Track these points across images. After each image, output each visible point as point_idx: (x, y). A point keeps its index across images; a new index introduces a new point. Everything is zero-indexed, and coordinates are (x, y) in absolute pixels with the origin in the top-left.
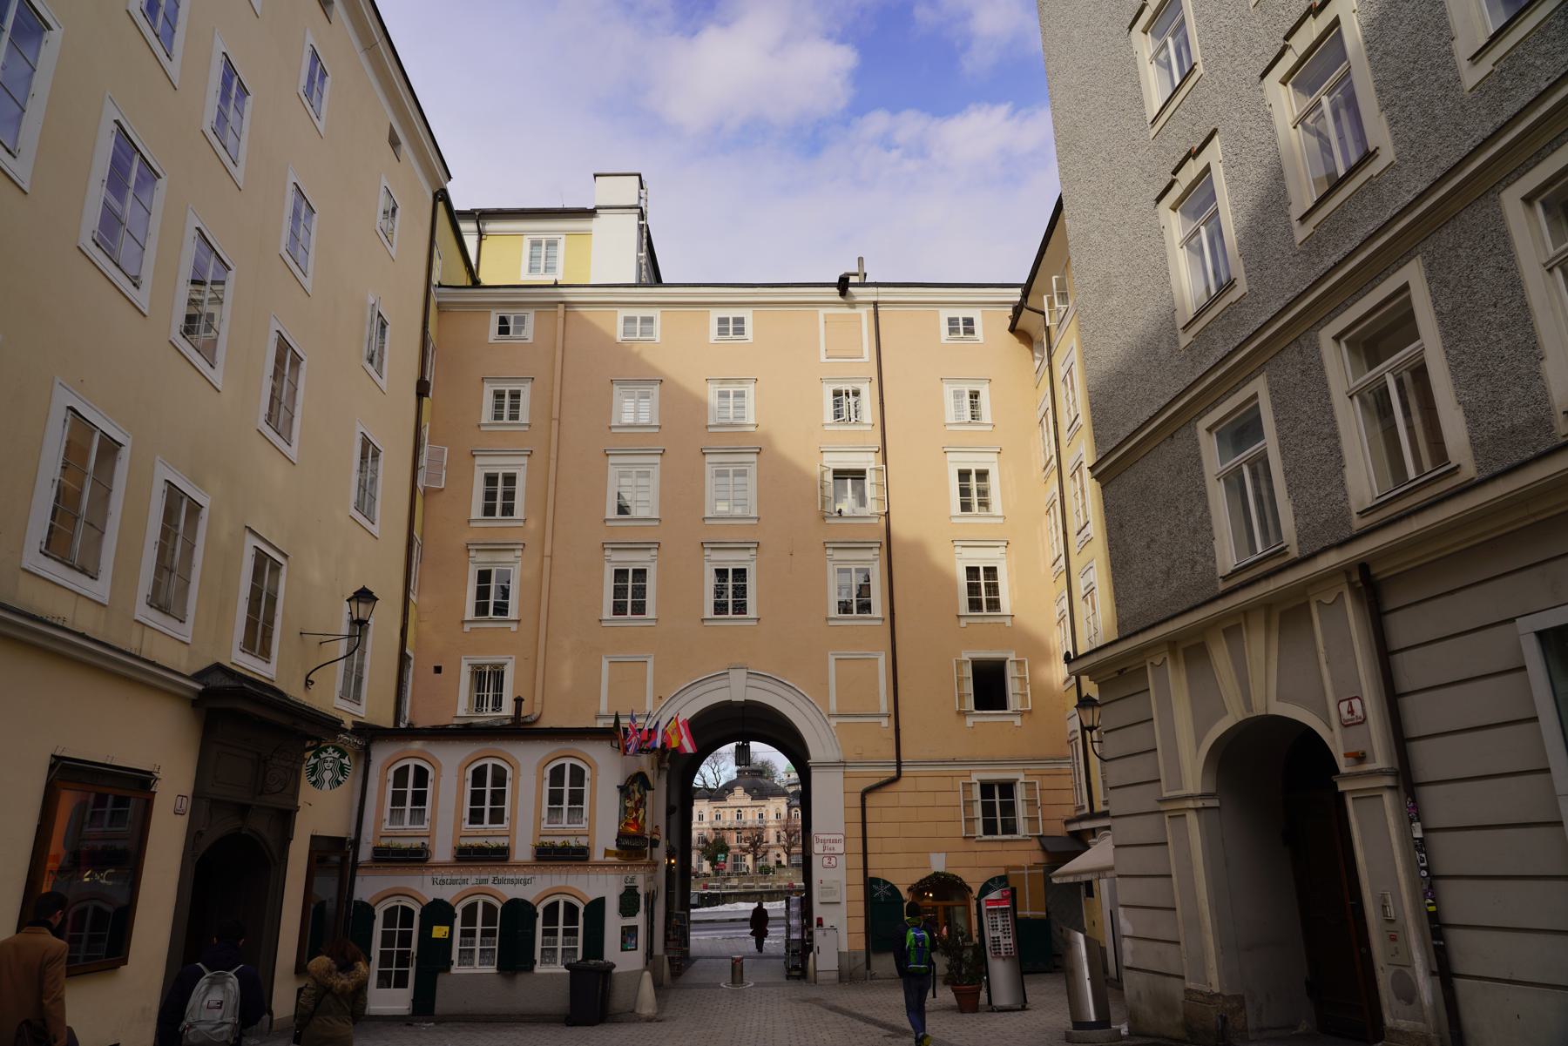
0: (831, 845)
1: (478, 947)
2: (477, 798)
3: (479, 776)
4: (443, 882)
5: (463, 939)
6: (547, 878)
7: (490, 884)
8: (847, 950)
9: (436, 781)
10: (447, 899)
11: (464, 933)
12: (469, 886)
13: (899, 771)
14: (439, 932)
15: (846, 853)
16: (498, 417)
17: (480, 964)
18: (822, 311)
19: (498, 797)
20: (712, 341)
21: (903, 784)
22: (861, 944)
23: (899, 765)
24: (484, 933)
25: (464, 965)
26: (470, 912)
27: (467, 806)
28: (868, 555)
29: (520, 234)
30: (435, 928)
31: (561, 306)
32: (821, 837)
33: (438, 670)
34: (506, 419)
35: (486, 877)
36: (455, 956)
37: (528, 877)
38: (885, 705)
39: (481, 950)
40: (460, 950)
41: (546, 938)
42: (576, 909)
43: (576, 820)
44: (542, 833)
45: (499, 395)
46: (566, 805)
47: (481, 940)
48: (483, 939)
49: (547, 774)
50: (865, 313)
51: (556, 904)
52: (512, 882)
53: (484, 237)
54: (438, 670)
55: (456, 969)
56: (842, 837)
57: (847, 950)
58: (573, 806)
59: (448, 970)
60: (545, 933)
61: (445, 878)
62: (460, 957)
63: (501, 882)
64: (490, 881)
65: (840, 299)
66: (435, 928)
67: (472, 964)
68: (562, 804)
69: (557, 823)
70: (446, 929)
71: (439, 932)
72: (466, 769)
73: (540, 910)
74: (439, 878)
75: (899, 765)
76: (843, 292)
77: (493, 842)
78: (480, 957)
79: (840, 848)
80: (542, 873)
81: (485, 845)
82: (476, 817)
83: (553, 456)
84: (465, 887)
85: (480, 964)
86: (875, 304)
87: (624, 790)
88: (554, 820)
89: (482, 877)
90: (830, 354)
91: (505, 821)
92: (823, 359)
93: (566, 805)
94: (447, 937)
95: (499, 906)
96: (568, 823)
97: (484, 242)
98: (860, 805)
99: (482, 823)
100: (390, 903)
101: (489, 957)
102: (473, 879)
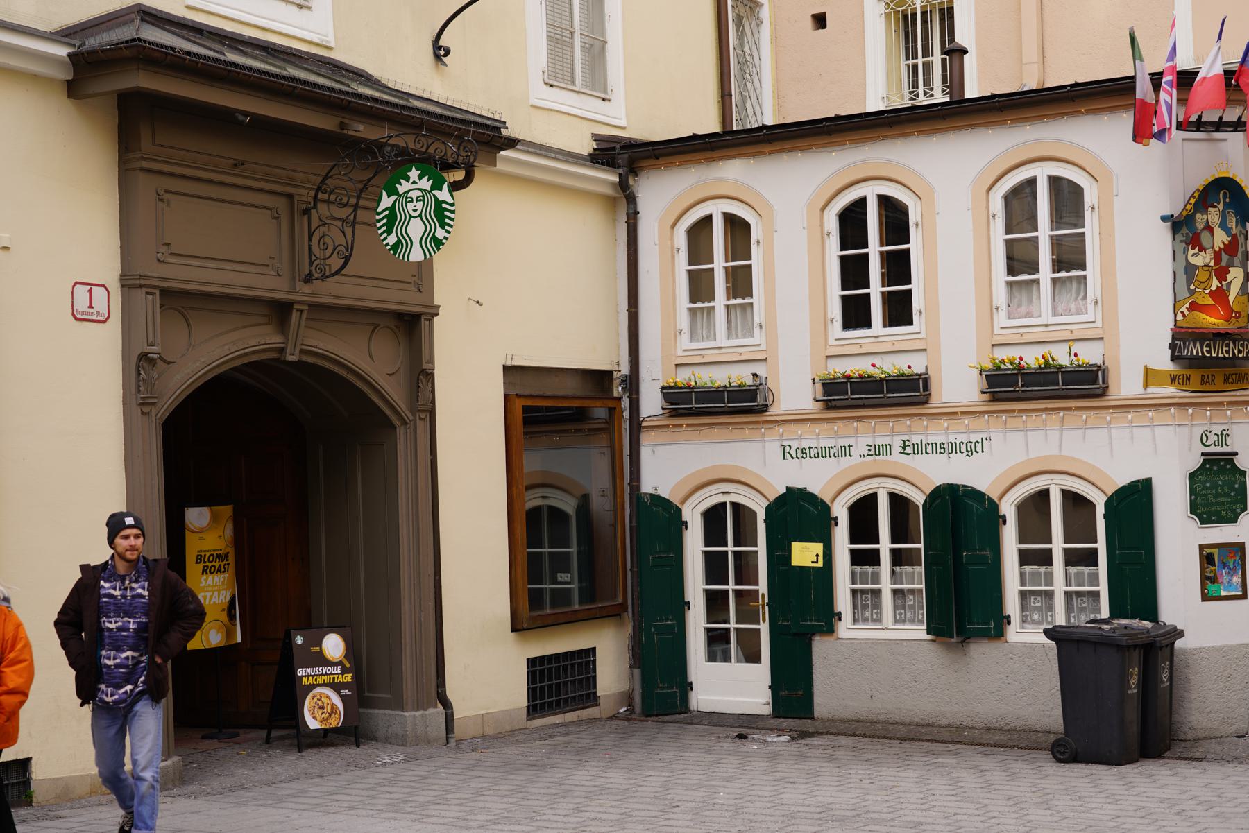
1: (886, 586)
2: (854, 271)
3: (852, 221)
4: (804, 453)
5: (858, 569)
6: (1016, 438)
7: (896, 456)
10: (814, 488)
11: (858, 558)
12: (856, 460)
14: (804, 554)
17: (896, 621)
19: (898, 267)
24: (898, 558)
25: (865, 620)
26: (863, 512)
27: (835, 291)
30: (796, 546)
35: (886, 440)
36: (843, 602)
37: (975, 437)
39: (895, 592)
40: (854, 592)
41: (1028, 569)
43: (1073, 306)
44: (997, 340)
46: (1045, 271)
47: (893, 572)
48: (897, 569)
49: (997, 206)
51: (1044, 495)
52: (940, 448)
55: (845, 628)
58: (1063, 274)
59: (830, 630)
60: (1026, 558)
61: (805, 444)
62: (855, 606)
63: (919, 449)
64: (897, 448)
66: (796, 546)
67: (878, 620)
68: (1037, 270)
69: (1029, 315)
70: (818, 548)
71: (804, 554)
73: (1008, 509)
74: (795, 445)
77: (891, 366)
78: (895, 607)
80: (1005, 429)
81: (872, 371)
82: (856, 314)
84: (845, 462)
85: (896, 621)
88: (1024, 309)
89: (880, 441)
91: (915, 318)
93: (1045, 271)
94: (820, 564)
95: (919, 499)
96: (1055, 314)
99: (867, 324)
101: (912, 607)
102: (860, 445)
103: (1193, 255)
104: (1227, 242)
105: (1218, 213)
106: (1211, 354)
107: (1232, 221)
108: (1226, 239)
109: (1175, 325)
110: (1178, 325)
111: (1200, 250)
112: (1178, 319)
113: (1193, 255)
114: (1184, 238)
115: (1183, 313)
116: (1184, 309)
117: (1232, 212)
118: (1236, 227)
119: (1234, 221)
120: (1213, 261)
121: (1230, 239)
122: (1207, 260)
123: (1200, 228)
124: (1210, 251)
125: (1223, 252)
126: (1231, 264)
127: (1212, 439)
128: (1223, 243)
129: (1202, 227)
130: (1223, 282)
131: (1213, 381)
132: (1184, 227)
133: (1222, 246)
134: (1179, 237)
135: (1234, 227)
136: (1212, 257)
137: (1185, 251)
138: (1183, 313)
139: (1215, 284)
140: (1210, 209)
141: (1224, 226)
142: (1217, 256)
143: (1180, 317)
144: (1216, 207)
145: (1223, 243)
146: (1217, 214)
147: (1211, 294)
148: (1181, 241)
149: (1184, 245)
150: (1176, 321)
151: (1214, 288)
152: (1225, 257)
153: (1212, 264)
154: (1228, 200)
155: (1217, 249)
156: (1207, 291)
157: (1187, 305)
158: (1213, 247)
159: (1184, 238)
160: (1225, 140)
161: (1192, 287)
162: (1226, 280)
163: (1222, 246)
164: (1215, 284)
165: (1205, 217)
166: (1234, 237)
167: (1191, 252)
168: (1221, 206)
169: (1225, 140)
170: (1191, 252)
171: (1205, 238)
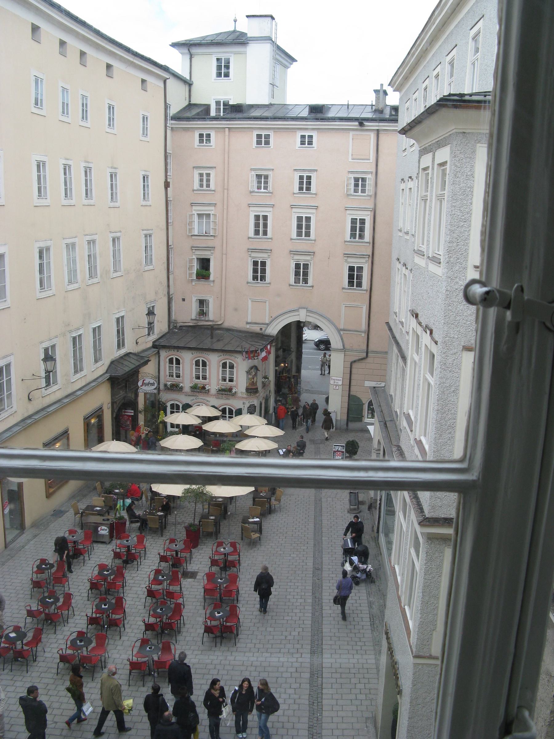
0: (337, 381)
8: (339, 419)
9: (183, 362)
13: (367, 355)
15: (342, 385)
16: (201, 186)
18: (351, 133)
20: (297, 148)
21: (369, 360)
22: (345, 417)
23: (367, 353)
28: (363, 260)
29: (210, 54)
31: (227, 130)
32: (333, 378)
33: (184, 300)
34: (205, 187)
38: (364, 327)
42: (233, 411)
45: (201, 175)
50: (373, 136)
53: (193, 56)
54: (184, 300)
56: (341, 379)
57: (339, 419)
65: (359, 128)
75: (367, 353)
76: (361, 124)
79: (340, 383)
83: (225, 207)
86: (378, 130)
87: (248, 372)
90: (354, 157)
92: (350, 160)
97: (193, 59)
98: (349, 367)
100: (172, 402)
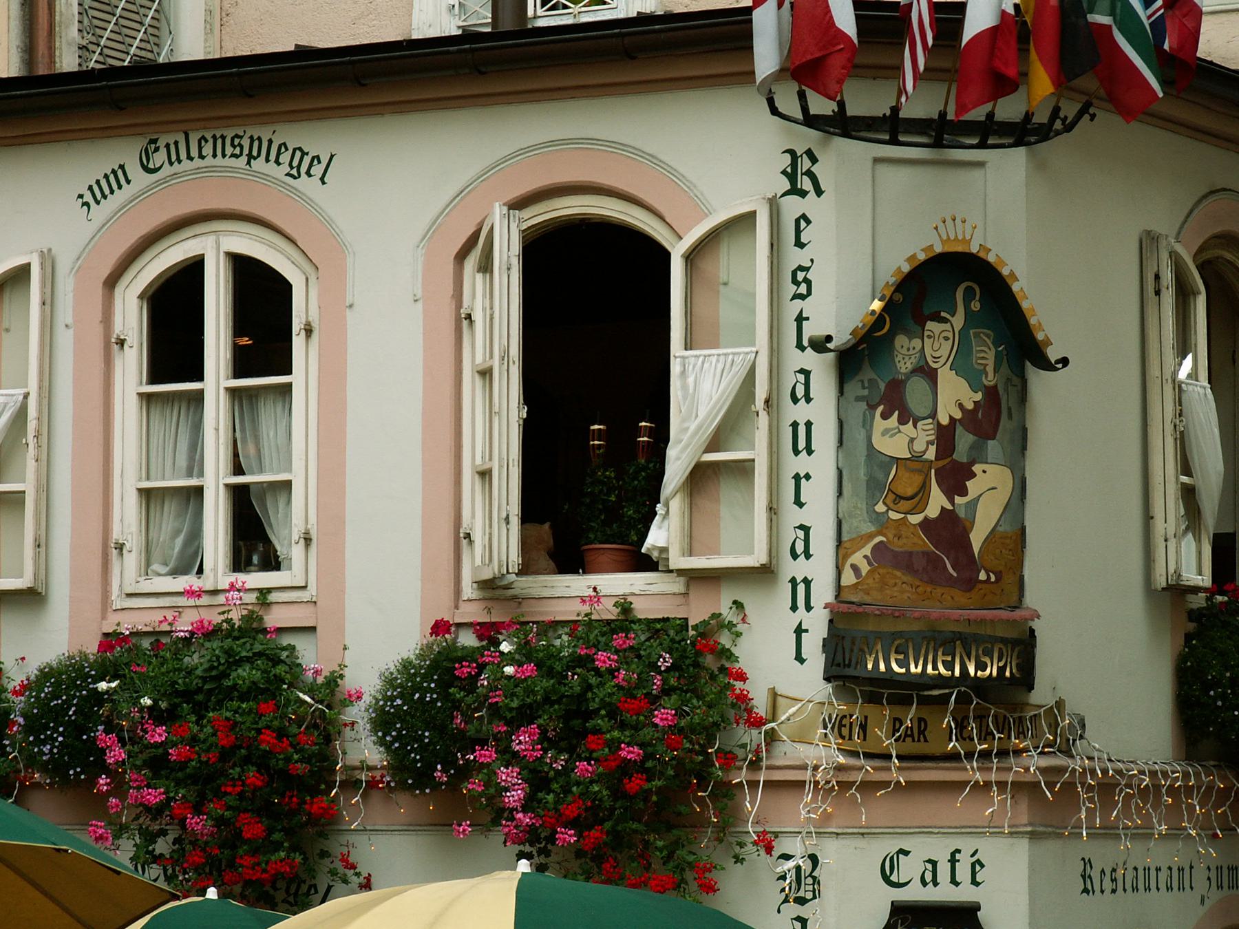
72: (111, 282)
103: (885, 432)
104: (970, 406)
105: (950, 335)
106: (908, 670)
107: (986, 355)
108: (971, 398)
109: (837, 597)
110: (846, 596)
111: (902, 421)
112: (844, 582)
113: (885, 432)
114: (866, 392)
115: (855, 568)
116: (858, 558)
117: (988, 336)
118: (996, 371)
119: (991, 355)
120: (933, 449)
121: (979, 396)
122: (919, 446)
123: (903, 370)
124: (927, 426)
125: (959, 430)
126: (978, 455)
127: (909, 869)
128: (961, 406)
129: (910, 366)
130: (958, 500)
131: (921, 732)
132: (866, 363)
133: (958, 415)
134: (853, 388)
135: (990, 369)
136: (933, 437)
137: (868, 425)
138: (855, 568)
139: (937, 502)
140: (930, 325)
141: (962, 365)
142: (945, 437)
143: (848, 578)
144: (945, 321)
145: (961, 406)
146: (946, 339)
147: (926, 524)
148: (858, 399)
149: (863, 405)
150: (839, 588)
151: (933, 511)
152: (964, 441)
153: (931, 454)
154: (976, 306)
155: (945, 421)
156: (915, 519)
157: (867, 551)
158: (933, 415)
159: (866, 392)
160: (981, 164)
161: (881, 508)
162: (964, 492)
163: (958, 415)
164: (937, 502)
165: (917, 343)
166: (992, 394)
167: (879, 424)
168: (958, 321)
169: (981, 164)
170: (879, 424)
171: (916, 392)
